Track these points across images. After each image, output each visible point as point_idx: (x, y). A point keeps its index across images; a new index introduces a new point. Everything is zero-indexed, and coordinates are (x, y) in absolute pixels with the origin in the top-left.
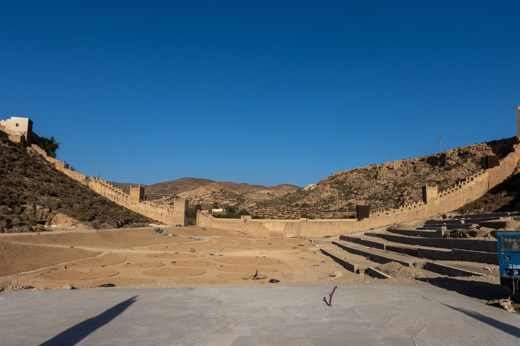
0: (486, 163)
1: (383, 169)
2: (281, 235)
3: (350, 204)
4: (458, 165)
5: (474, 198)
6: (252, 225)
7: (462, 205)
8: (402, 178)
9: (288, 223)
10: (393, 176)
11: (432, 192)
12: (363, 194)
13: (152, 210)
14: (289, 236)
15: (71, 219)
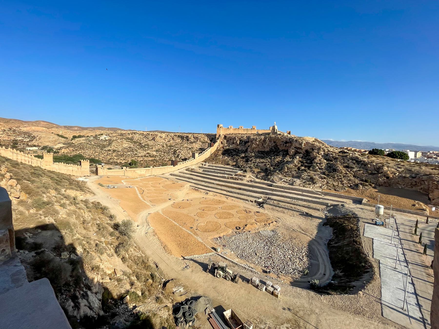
0: (210, 146)
1: (158, 137)
2: (144, 175)
3: (148, 153)
4: (194, 142)
5: (207, 157)
6: (130, 172)
7: (204, 159)
8: (169, 143)
9: (147, 170)
10: (164, 141)
11: (197, 155)
12: (152, 149)
13: (65, 168)
14: (147, 175)
15: (79, 192)
